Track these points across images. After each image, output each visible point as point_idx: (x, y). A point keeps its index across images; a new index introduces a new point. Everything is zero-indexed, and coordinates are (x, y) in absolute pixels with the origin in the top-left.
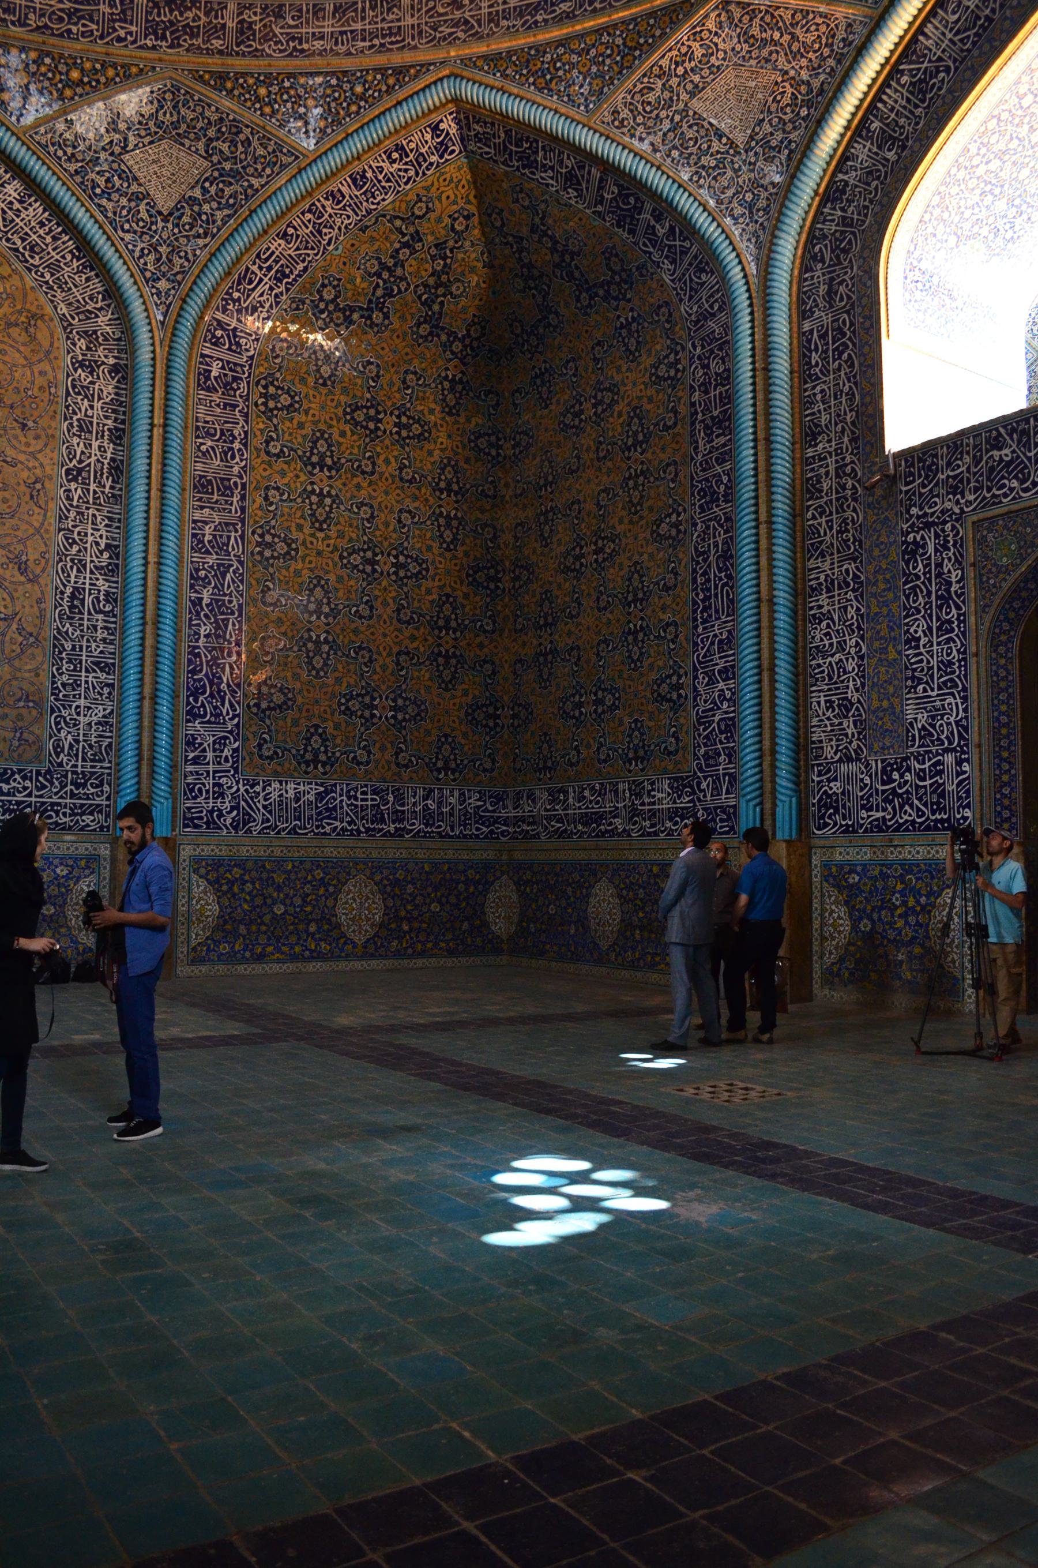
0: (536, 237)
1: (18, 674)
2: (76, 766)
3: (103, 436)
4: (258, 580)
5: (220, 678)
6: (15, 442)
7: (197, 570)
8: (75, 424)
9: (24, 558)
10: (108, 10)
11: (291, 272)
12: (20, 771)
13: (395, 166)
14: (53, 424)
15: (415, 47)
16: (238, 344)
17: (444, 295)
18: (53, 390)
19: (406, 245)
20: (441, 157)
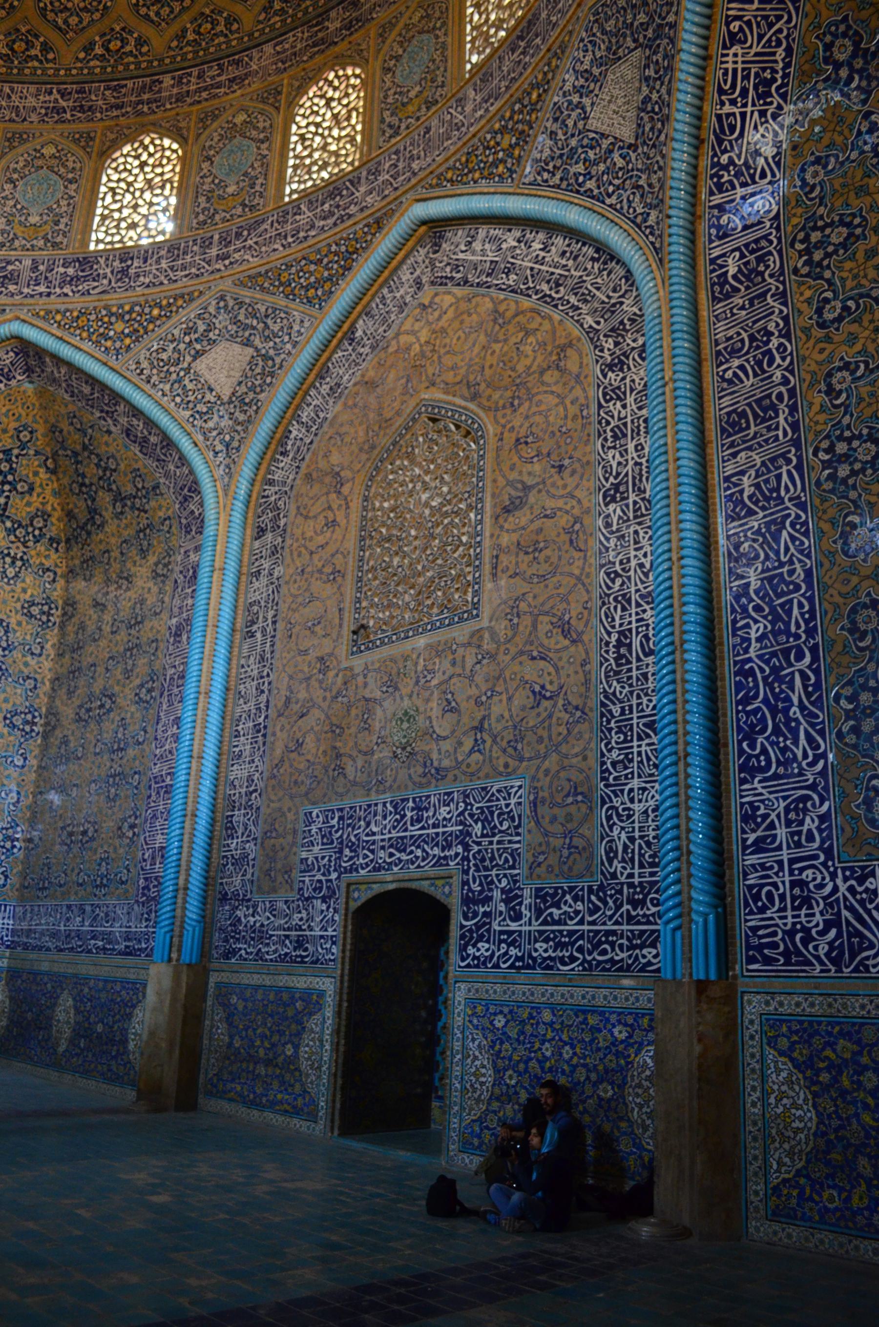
1: (566, 762)
2: (631, 876)
4: (833, 523)
5: (788, 699)
7: (737, 547)
9: (567, 618)
11: (774, 71)
12: (572, 889)
14: (588, 449)
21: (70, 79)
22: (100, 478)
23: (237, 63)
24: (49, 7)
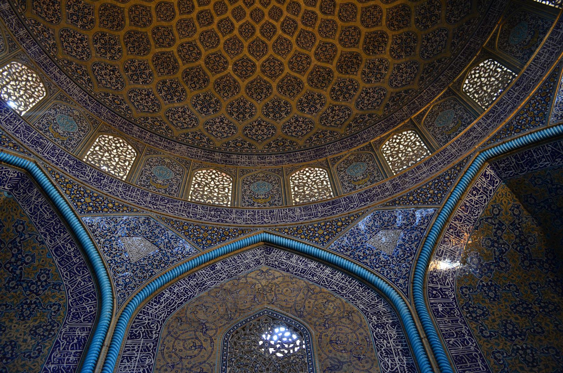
0: (553, 194)
3: (399, 354)
6: (357, 367)
8: (383, 352)
10: (344, 203)
13: (477, 197)
15: (461, 154)
16: (445, 294)
17: (527, 245)
18: (368, 340)
19: (498, 229)
20: (493, 186)
21: (95, 98)
22: (10, 263)
23: (169, 143)
24: (96, 71)
